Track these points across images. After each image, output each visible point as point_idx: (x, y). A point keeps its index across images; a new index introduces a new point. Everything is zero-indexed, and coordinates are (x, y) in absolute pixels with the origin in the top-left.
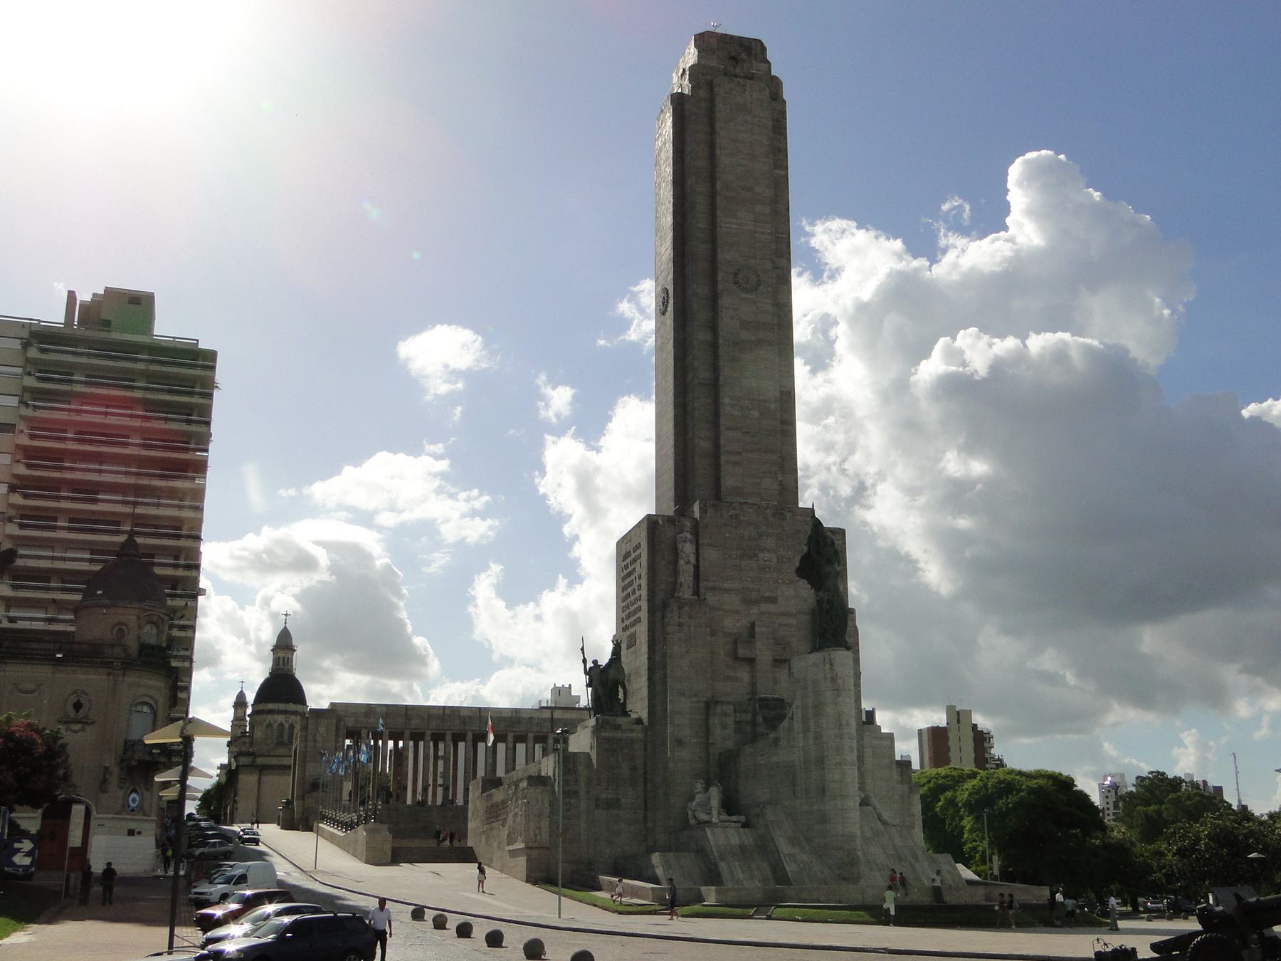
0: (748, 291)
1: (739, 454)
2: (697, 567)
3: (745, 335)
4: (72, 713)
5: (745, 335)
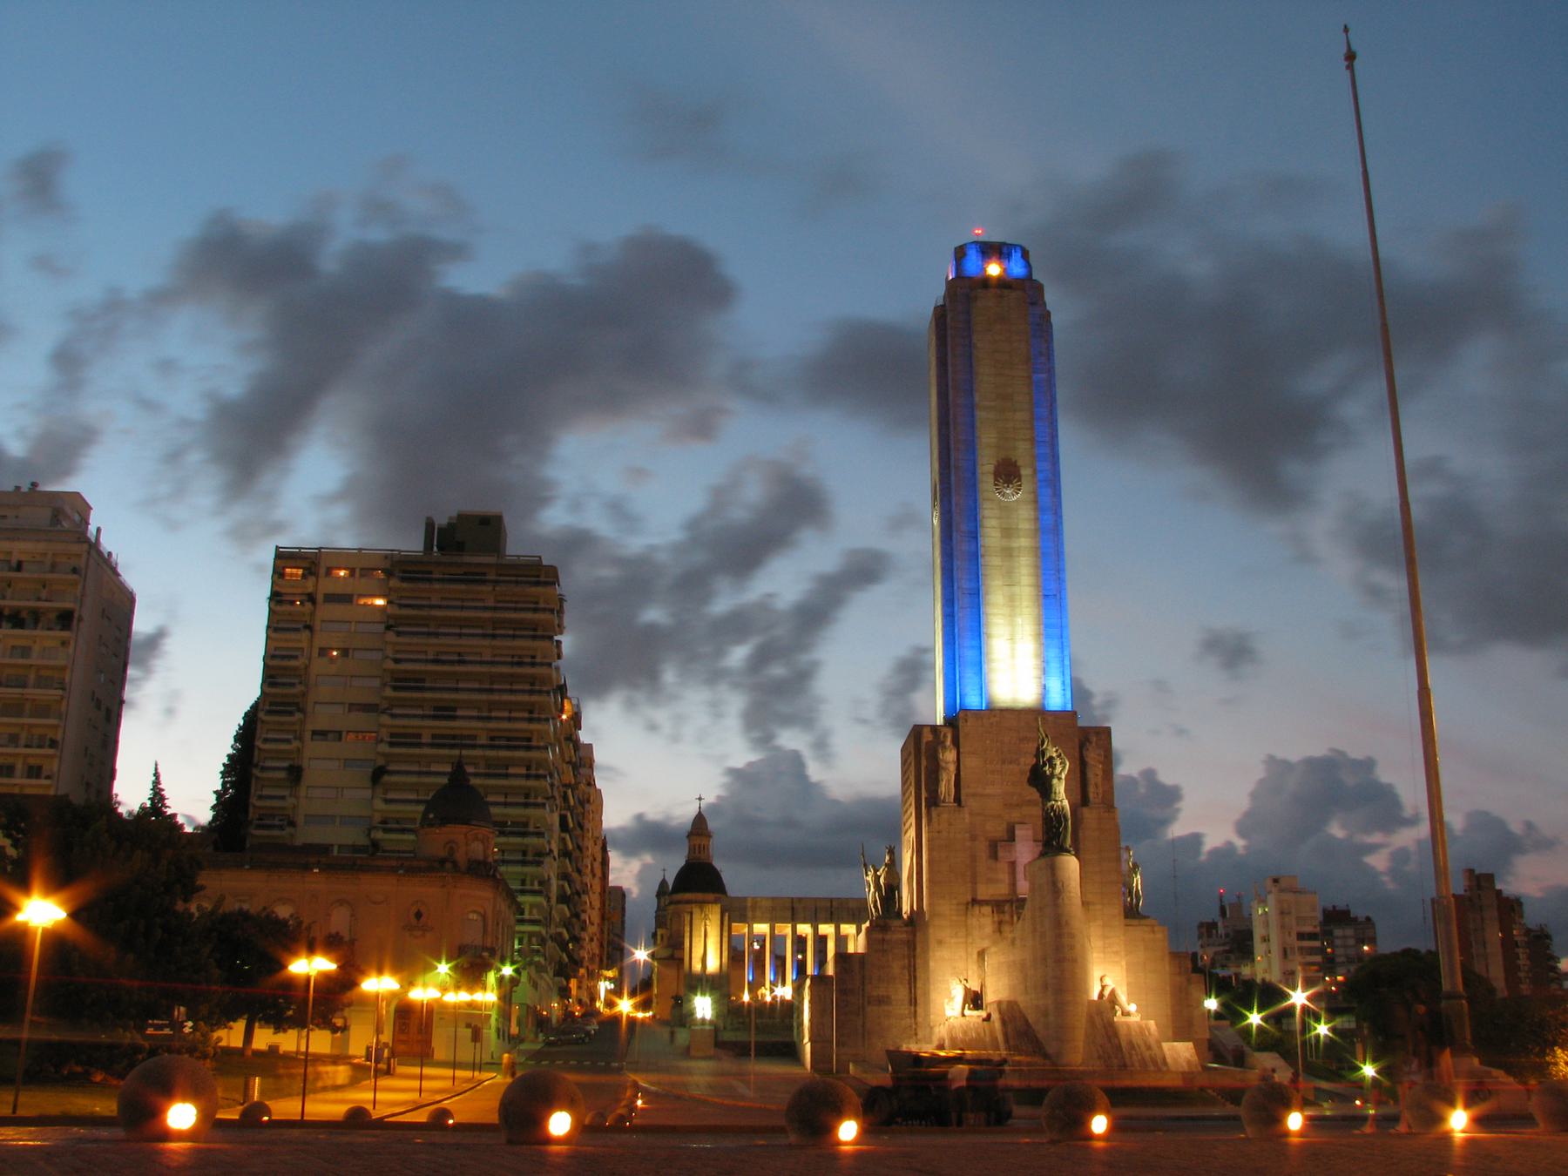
2: (958, 776)
4: (413, 920)
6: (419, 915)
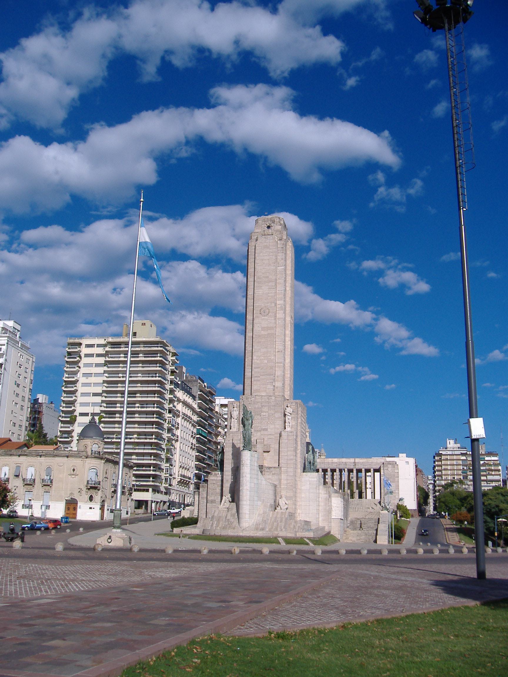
0: (264, 316)
1: (259, 377)
3: (263, 333)
5: (263, 333)
6: (74, 470)
